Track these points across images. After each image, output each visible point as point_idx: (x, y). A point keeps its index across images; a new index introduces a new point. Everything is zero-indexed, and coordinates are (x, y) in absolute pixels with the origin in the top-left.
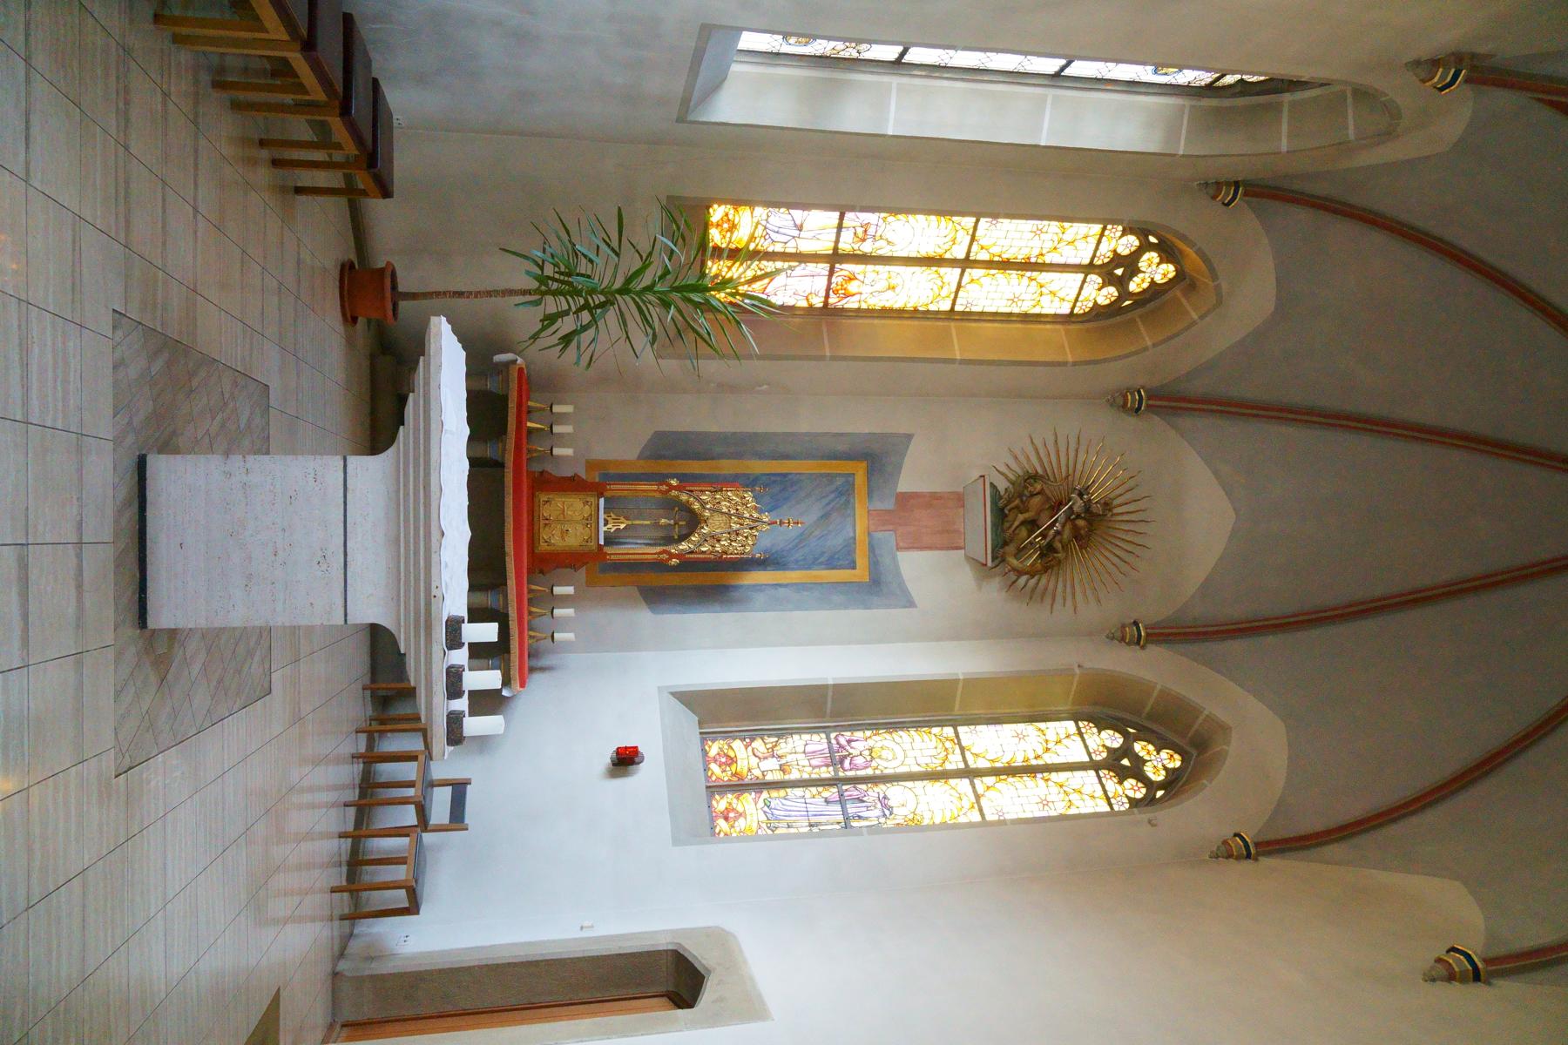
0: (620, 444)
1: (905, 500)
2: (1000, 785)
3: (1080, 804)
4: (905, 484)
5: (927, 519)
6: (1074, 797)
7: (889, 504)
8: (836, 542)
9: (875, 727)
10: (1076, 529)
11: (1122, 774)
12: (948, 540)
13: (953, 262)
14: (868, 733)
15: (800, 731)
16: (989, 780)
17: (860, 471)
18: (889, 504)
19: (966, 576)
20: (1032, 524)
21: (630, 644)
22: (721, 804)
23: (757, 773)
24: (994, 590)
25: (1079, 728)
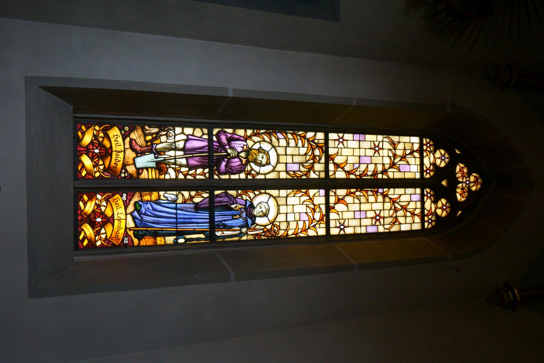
2: (349, 199)
3: (402, 220)
6: (401, 213)
14: (249, 132)
15: (183, 125)
16: (341, 192)
23: (131, 169)
25: (421, 144)
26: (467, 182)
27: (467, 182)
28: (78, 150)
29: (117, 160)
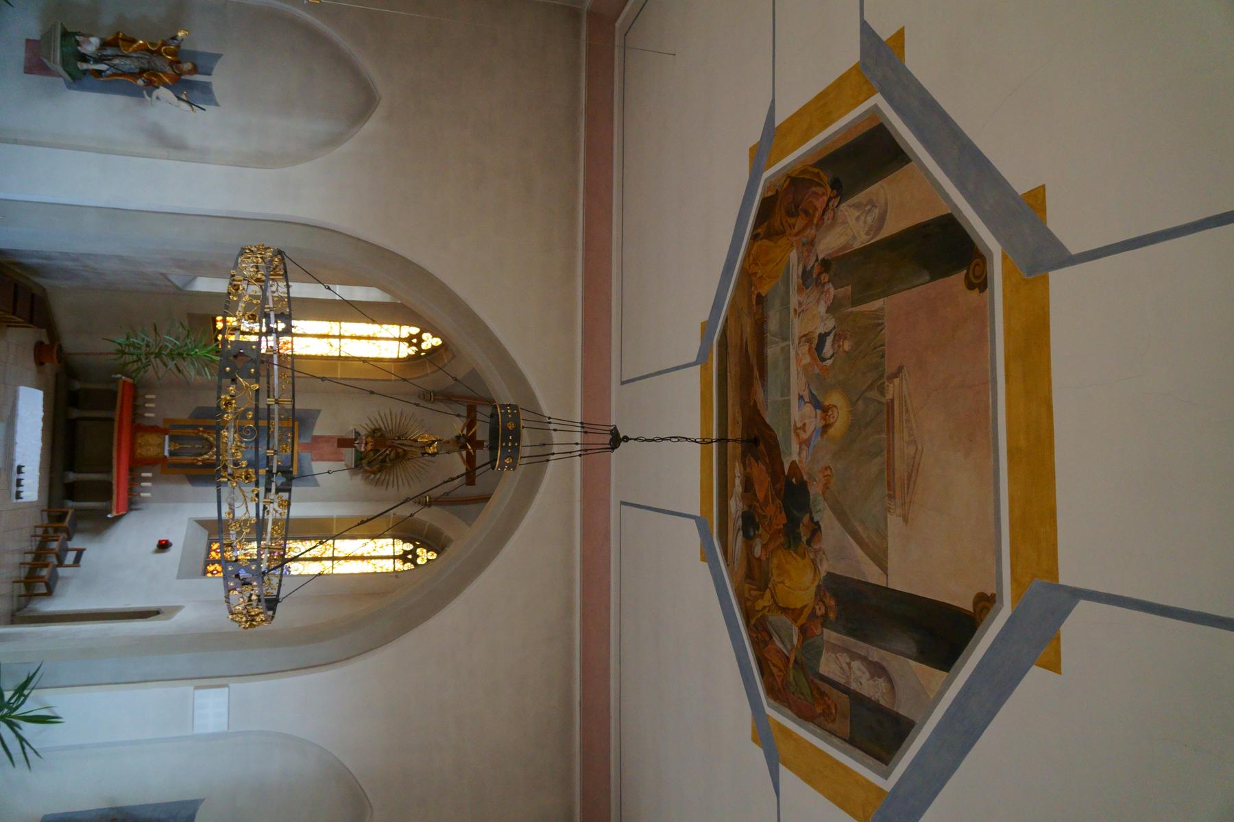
0: (180, 411)
1: (316, 439)
4: (317, 432)
7: (308, 440)
13: (334, 337)
18: (308, 440)
24: (358, 481)
26: (424, 556)
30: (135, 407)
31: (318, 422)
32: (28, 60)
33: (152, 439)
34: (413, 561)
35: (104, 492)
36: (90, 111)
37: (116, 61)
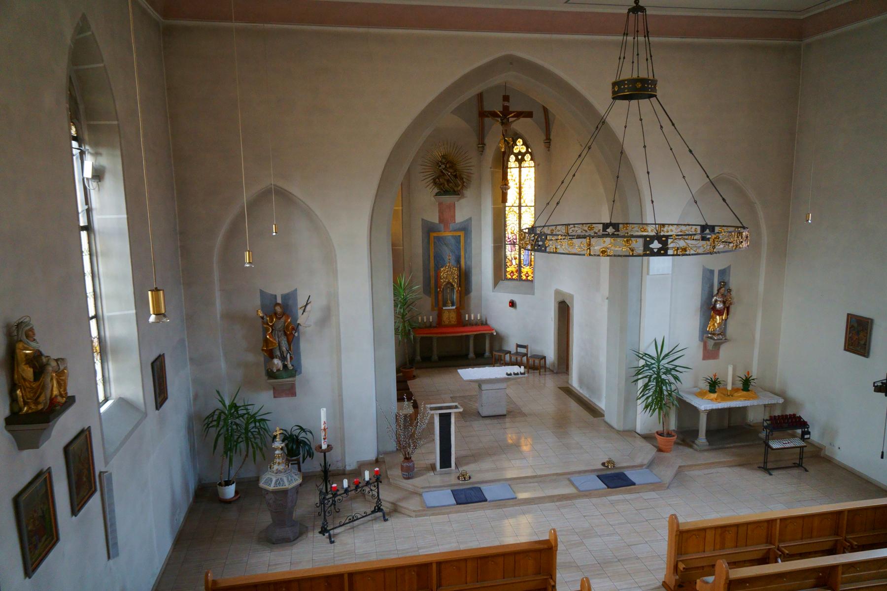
0: (427, 302)
1: (441, 221)
4: (437, 221)
5: (446, 214)
7: (442, 226)
8: (453, 241)
9: (505, 230)
10: (450, 167)
11: (523, 160)
12: (452, 207)
17: (433, 235)
18: (442, 226)
19: (463, 201)
20: (448, 181)
21: (480, 298)
22: (524, 277)
24: (468, 193)
26: (520, 147)
27: (520, 147)
28: (511, 279)
29: (514, 270)
30: (426, 327)
31: (429, 219)
32: (287, 395)
33: (445, 316)
34: (523, 155)
35: (480, 339)
36: (313, 359)
37: (284, 349)
